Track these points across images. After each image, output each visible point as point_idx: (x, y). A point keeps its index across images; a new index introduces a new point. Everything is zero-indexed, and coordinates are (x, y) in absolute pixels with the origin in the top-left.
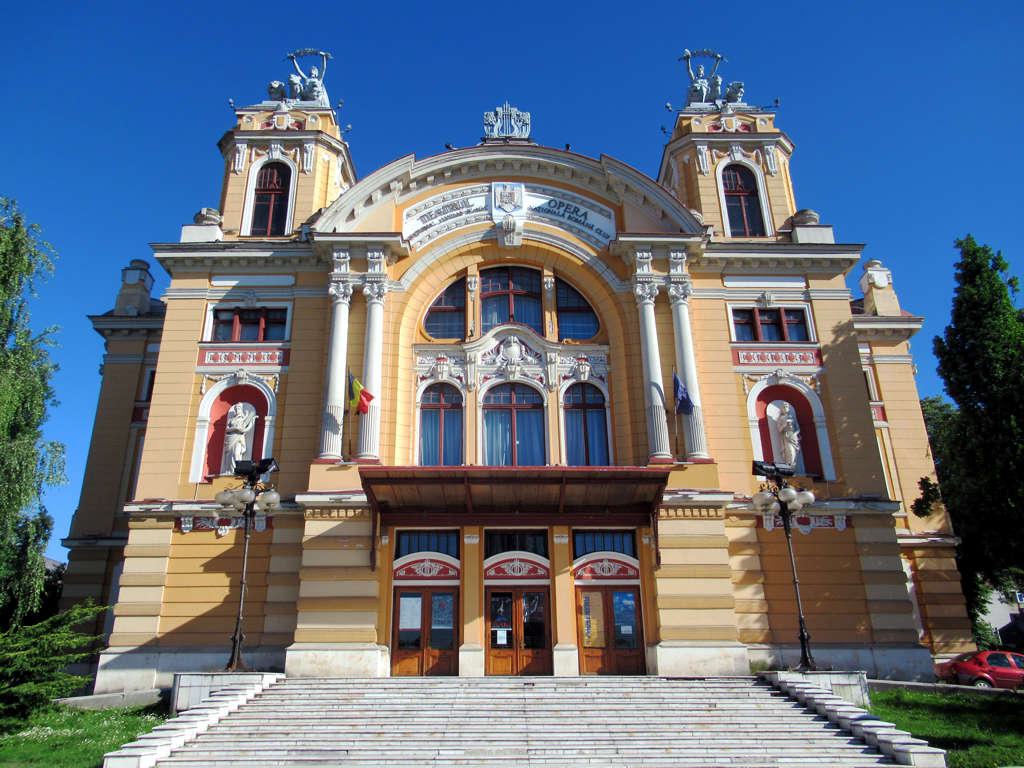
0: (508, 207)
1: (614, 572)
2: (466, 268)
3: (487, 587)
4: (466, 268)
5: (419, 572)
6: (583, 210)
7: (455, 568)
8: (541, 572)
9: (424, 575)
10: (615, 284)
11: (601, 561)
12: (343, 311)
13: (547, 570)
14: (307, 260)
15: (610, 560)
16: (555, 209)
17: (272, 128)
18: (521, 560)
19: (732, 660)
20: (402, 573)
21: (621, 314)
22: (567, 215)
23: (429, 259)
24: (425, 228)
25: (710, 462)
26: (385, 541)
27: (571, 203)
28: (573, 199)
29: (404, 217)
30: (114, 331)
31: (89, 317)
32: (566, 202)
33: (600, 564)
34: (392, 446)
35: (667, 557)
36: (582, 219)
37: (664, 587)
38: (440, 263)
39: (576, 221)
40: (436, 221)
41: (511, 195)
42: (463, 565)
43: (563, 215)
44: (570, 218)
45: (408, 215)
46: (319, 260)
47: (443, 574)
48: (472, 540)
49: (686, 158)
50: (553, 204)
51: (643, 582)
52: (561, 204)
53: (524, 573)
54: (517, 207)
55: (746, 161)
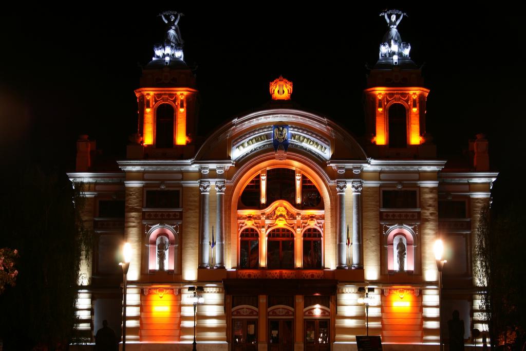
5: (242, 313)
7: (256, 311)
8: (291, 313)
9: (245, 314)
13: (293, 312)
18: (283, 308)
20: (235, 313)
48: (263, 300)
53: (284, 313)
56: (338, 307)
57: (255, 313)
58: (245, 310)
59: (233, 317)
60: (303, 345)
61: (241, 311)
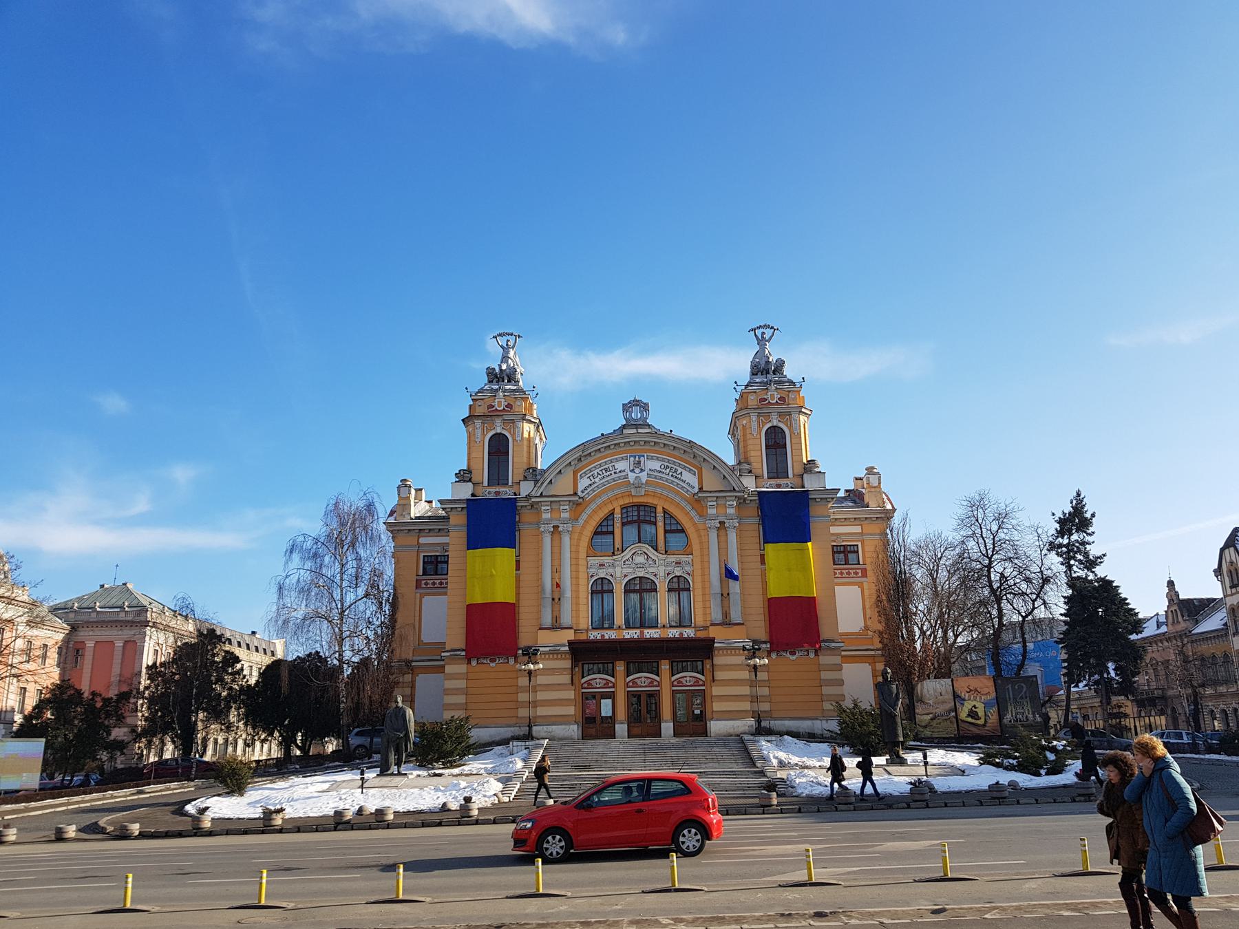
0: (637, 470)
2: (614, 509)
3: (628, 691)
4: (614, 509)
6: (680, 470)
10: (696, 519)
11: (686, 677)
12: (547, 540)
14: (526, 506)
15: (691, 677)
17: (494, 409)
19: (747, 727)
22: (671, 474)
24: (590, 485)
25: (743, 624)
26: (577, 669)
27: (673, 466)
28: (674, 463)
29: (579, 476)
32: (670, 465)
35: (719, 675)
36: (679, 476)
37: (716, 691)
38: (600, 507)
40: (597, 480)
41: (639, 462)
42: (616, 680)
45: (581, 477)
46: (532, 506)
47: (606, 685)
48: (620, 667)
49: (744, 422)
50: (663, 467)
51: (706, 687)
52: (667, 467)
54: (642, 470)
55: (781, 425)
58: (598, 681)
60: (672, 724)
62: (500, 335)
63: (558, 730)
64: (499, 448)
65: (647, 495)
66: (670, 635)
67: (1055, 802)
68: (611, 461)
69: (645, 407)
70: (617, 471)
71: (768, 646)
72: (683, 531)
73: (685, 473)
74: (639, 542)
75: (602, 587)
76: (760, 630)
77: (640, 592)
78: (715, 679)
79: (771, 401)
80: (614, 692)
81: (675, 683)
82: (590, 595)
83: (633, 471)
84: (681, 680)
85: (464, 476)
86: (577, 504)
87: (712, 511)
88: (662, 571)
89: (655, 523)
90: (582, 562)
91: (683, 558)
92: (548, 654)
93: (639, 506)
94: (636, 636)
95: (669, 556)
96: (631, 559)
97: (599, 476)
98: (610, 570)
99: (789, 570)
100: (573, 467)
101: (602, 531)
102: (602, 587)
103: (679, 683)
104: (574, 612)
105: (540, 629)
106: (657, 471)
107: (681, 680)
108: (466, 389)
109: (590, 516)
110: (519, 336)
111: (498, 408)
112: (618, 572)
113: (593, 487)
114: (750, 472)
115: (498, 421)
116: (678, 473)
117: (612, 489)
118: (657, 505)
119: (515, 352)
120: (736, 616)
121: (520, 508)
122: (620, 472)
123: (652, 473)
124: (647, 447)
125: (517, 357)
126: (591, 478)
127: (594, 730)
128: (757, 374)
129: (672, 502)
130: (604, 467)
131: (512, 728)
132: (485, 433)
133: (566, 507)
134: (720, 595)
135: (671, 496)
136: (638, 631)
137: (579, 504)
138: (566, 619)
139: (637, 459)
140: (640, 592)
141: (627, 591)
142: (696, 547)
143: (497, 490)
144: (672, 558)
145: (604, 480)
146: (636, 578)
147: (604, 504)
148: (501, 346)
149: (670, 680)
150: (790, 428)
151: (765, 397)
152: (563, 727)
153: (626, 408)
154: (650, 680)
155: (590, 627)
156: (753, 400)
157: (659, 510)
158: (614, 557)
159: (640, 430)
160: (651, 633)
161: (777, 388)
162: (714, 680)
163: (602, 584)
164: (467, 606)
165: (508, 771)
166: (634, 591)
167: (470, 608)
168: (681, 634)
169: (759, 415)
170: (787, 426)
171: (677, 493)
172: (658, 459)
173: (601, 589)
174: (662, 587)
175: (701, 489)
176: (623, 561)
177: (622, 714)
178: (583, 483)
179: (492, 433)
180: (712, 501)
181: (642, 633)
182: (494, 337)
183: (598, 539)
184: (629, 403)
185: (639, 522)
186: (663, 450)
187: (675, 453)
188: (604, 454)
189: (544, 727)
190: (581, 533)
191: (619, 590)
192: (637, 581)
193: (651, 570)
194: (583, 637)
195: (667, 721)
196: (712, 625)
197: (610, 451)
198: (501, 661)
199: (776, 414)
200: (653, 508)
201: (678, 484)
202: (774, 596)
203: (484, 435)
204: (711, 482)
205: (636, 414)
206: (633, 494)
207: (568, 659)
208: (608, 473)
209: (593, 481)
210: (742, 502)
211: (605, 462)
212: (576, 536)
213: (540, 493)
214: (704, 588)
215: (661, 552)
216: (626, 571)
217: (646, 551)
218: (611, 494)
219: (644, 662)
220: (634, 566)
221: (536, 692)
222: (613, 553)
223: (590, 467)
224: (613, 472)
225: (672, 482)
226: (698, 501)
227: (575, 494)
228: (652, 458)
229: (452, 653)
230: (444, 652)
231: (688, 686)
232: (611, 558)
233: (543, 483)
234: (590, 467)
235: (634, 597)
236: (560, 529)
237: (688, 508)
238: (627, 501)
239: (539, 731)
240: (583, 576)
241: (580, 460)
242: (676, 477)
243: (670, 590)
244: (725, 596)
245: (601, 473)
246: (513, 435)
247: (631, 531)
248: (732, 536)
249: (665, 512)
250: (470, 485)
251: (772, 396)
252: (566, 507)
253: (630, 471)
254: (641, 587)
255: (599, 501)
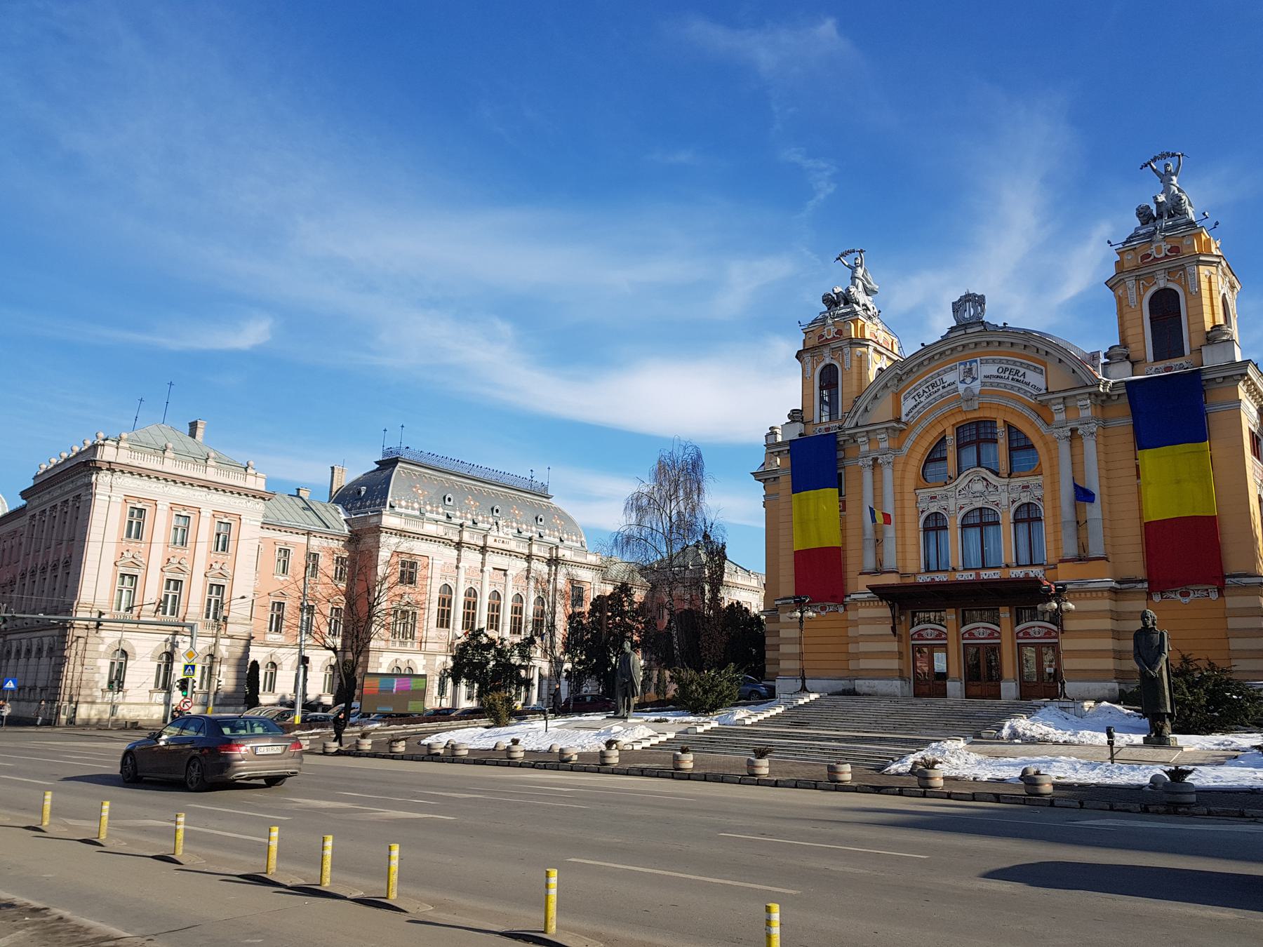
0: (968, 380)
1: (1042, 634)
6: (1022, 371)
8: (996, 635)
10: (1043, 429)
11: (1034, 627)
12: (868, 475)
15: (1039, 627)
16: (1002, 374)
17: (824, 338)
21: (1049, 451)
22: (1011, 377)
23: (918, 430)
24: (916, 406)
30: (766, 479)
31: (752, 473)
32: (1010, 367)
33: (1033, 629)
34: (904, 559)
37: (1066, 644)
38: (926, 431)
39: (1017, 380)
40: (922, 399)
41: (970, 369)
43: (1008, 378)
44: (1013, 379)
45: (905, 399)
47: (938, 637)
50: (1000, 370)
52: (1005, 371)
54: (974, 379)
55: (1171, 285)
56: (1064, 622)
57: (943, 636)
58: (929, 631)
59: (914, 642)
61: (924, 633)
62: (842, 255)
63: (881, 686)
64: (829, 379)
65: (983, 407)
66: (1013, 576)
67: (1111, 809)
68: (939, 375)
69: (979, 301)
70: (946, 385)
71: (1146, 585)
72: (1032, 447)
73: (1028, 373)
74: (979, 465)
75: (936, 524)
76: (1134, 565)
77: (982, 525)
78: (1065, 629)
79: (1156, 256)
80: (1057, 643)
81: (1021, 635)
82: (921, 534)
83: (963, 382)
84: (1027, 630)
85: (795, 416)
86: (901, 431)
87: (1060, 417)
88: (1004, 498)
89: (996, 441)
90: (909, 497)
91: (1032, 481)
92: (868, 601)
93: (979, 424)
94: (972, 578)
95: (1012, 480)
96: (967, 488)
97: (926, 394)
98: (943, 503)
99: (1178, 482)
100: (890, 390)
101: (935, 456)
102: (936, 524)
103: (1026, 634)
104: (900, 555)
105: (861, 574)
106: (994, 376)
107: (1027, 630)
108: (799, 322)
109: (916, 443)
110: (862, 251)
111: (828, 338)
112: (952, 504)
113: (919, 407)
114: (1128, 357)
115: (826, 351)
116: (1020, 374)
117: (938, 407)
118: (995, 418)
119: (865, 270)
120: (1096, 549)
121: (842, 443)
122: (949, 385)
123: (988, 380)
124: (978, 350)
125: (869, 274)
126: (917, 398)
127: (927, 687)
128: (1148, 223)
129: (1013, 411)
130: (931, 382)
131: (843, 682)
132: (815, 367)
133: (883, 436)
134: (1075, 523)
135: (1011, 404)
136: (973, 573)
137: (902, 430)
138: (890, 561)
139: (968, 366)
140: (982, 525)
141: (964, 526)
142: (1045, 465)
143: (827, 426)
144: (1017, 482)
145: (930, 399)
146: (973, 510)
147: (932, 426)
148: (849, 266)
149: (1012, 630)
150: (1185, 288)
151: (1149, 252)
152: (886, 682)
153: (957, 307)
154: (989, 631)
155: (923, 571)
156: (1131, 260)
157: (1000, 423)
158: (946, 487)
159: (969, 331)
160: (986, 575)
161: (1165, 237)
162: (1063, 631)
163: (936, 520)
164: (795, 552)
165: (725, 722)
166: (973, 526)
167: (797, 553)
168: (1027, 574)
169: (1138, 279)
170: (1180, 284)
171: (1018, 400)
172: (994, 361)
173: (934, 525)
174: (1006, 518)
175: (1047, 389)
176: (957, 491)
177: (957, 670)
178: (907, 405)
179: (822, 364)
180: (1059, 404)
181: (978, 575)
182: (837, 259)
183: (932, 468)
184: (960, 300)
185: (978, 442)
186: (975, 351)
187: (1015, 350)
188: (928, 367)
189: (867, 682)
190: (906, 463)
191: (954, 523)
192: (978, 513)
193: (992, 498)
194: (911, 580)
195: (1008, 681)
196: (1062, 561)
197: (936, 363)
198: (831, 610)
199: (1163, 271)
200: (993, 423)
201: (1019, 389)
202: (1153, 519)
203: (814, 369)
204: (1059, 381)
205: (970, 312)
206: (964, 410)
207: (885, 607)
208: (936, 389)
209: (918, 401)
210: (1103, 401)
211: (931, 377)
212: (899, 467)
213: (855, 421)
214: (1054, 515)
215: (1004, 476)
216: (962, 502)
217: (985, 476)
218: (938, 413)
219: (984, 609)
220: (971, 495)
221: (858, 643)
222: (946, 483)
223: (914, 386)
224: (940, 387)
225: (1012, 387)
226: (1042, 409)
227: (898, 420)
228: (987, 362)
229: (784, 601)
230: (776, 600)
231: (1038, 638)
232: (942, 488)
233: (856, 412)
234: (914, 386)
235: (974, 534)
236: (879, 461)
237: (1033, 417)
238: (960, 418)
239: (861, 686)
240: (910, 512)
241: (900, 380)
242: (1017, 380)
243: (1017, 521)
244: (1080, 524)
245: (927, 390)
246: (842, 365)
247: (970, 455)
248: (1090, 446)
249: (1010, 427)
250: (798, 424)
251: (1159, 250)
252: (883, 436)
253: (961, 382)
254: (981, 521)
255: (925, 424)
